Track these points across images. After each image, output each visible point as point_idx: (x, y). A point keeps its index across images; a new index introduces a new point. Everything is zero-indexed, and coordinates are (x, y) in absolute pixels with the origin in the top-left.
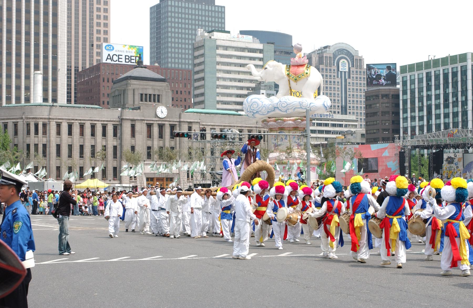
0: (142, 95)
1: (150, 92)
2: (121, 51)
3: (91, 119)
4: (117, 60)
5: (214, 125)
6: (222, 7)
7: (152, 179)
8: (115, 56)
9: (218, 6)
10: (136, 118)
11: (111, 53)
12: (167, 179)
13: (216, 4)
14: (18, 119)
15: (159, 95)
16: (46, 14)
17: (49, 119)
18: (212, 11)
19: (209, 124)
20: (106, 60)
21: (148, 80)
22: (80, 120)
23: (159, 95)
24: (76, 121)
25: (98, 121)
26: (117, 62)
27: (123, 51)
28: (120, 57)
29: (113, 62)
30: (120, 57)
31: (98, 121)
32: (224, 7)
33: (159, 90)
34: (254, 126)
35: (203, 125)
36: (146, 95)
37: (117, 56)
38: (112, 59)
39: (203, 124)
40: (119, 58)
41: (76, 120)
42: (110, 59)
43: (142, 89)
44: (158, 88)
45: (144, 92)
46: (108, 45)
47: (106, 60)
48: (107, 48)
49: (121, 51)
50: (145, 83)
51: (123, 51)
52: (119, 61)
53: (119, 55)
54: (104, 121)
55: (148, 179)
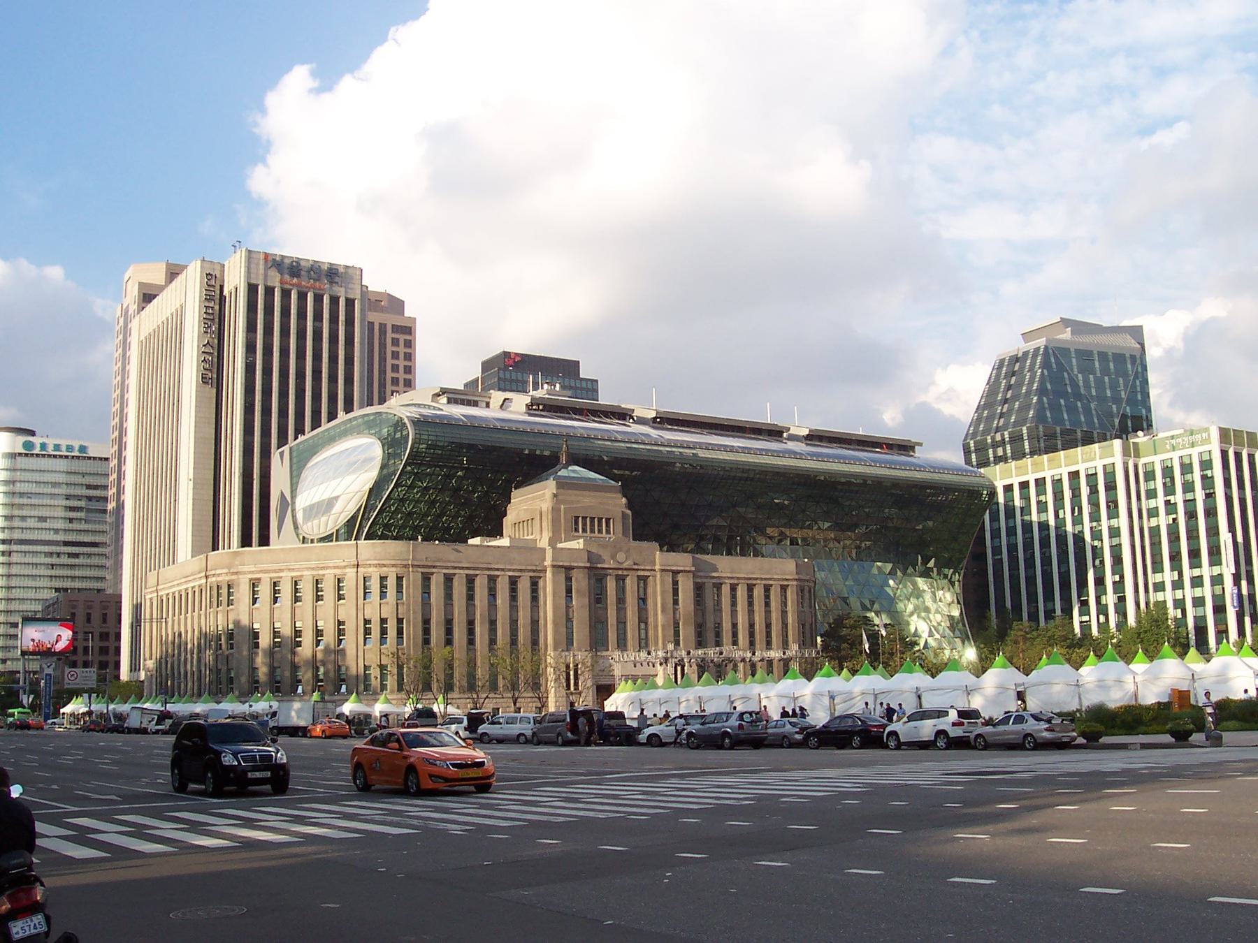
3: (489, 566)
14: (345, 567)
16: (333, 379)
22: (468, 568)
23: (608, 520)
24: (461, 571)
25: (503, 570)
31: (503, 570)
32: (597, 381)
35: (701, 577)
41: (462, 568)
54: (514, 570)
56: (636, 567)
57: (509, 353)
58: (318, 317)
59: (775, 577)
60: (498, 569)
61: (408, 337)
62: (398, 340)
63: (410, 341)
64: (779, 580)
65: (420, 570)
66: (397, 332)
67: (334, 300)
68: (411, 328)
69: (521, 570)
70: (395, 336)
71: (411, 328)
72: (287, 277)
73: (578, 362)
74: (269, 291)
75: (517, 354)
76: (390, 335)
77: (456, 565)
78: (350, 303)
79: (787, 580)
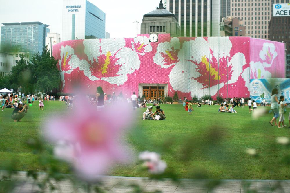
1: (158, 24)
2: (286, 8)
4: (283, 14)
7: (148, 88)
8: (282, 12)
11: (279, 10)
12: (160, 88)
15: (164, 26)
20: (276, 15)
21: (156, 17)
26: (284, 15)
27: (288, 8)
28: (286, 12)
29: (281, 16)
30: (286, 12)
33: (164, 23)
36: (154, 27)
37: (283, 11)
38: (280, 14)
40: (285, 13)
42: (279, 13)
43: (151, 23)
44: (164, 21)
45: (153, 25)
46: (277, 5)
47: (276, 15)
48: (277, 7)
49: (286, 8)
50: (156, 19)
51: (288, 8)
52: (285, 15)
53: (285, 11)
55: (144, 88)
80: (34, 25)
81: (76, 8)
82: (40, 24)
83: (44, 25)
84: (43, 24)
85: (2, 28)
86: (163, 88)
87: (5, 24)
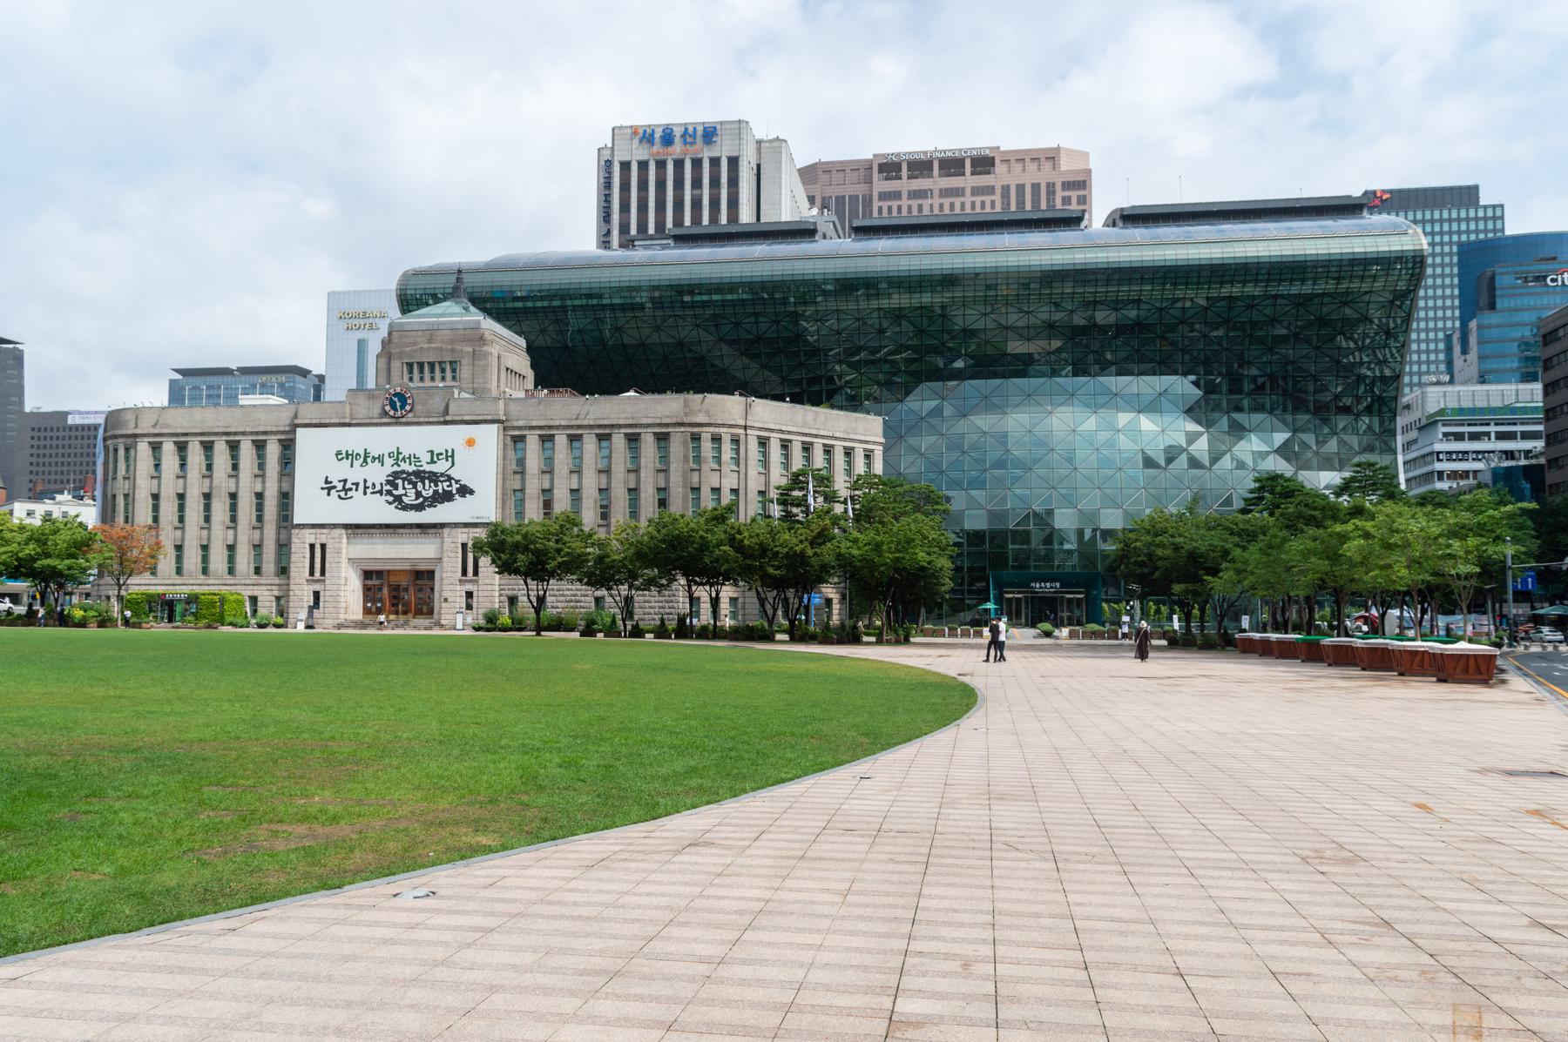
0: (410, 365)
5: (550, 427)
6: (1494, 207)
7: (379, 574)
9: (1485, 207)
10: (327, 421)
13: (1482, 202)
17: (135, 436)
18: (1477, 219)
19: (534, 424)
31: (243, 433)
34: (674, 421)
39: (516, 424)
54: (257, 433)
56: (416, 420)
57: (1374, 192)
58: (697, 183)
59: (644, 421)
60: (236, 434)
61: (1081, 193)
62: (1070, 197)
63: (1085, 197)
64: (648, 426)
65: (146, 439)
66: (1069, 189)
67: (715, 162)
68: (1084, 182)
69: (265, 433)
70: (1067, 194)
71: (1084, 182)
72: (657, 148)
73: (1476, 188)
74: (643, 165)
75: (1384, 192)
76: (1060, 194)
77: (185, 431)
78: (734, 162)
79: (667, 425)
80: (279, 376)
81: (371, 320)
82: (304, 373)
83: (316, 376)
84: (314, 373)
85: (172, 383)
86: (431, 574)
87: (185, 373)
